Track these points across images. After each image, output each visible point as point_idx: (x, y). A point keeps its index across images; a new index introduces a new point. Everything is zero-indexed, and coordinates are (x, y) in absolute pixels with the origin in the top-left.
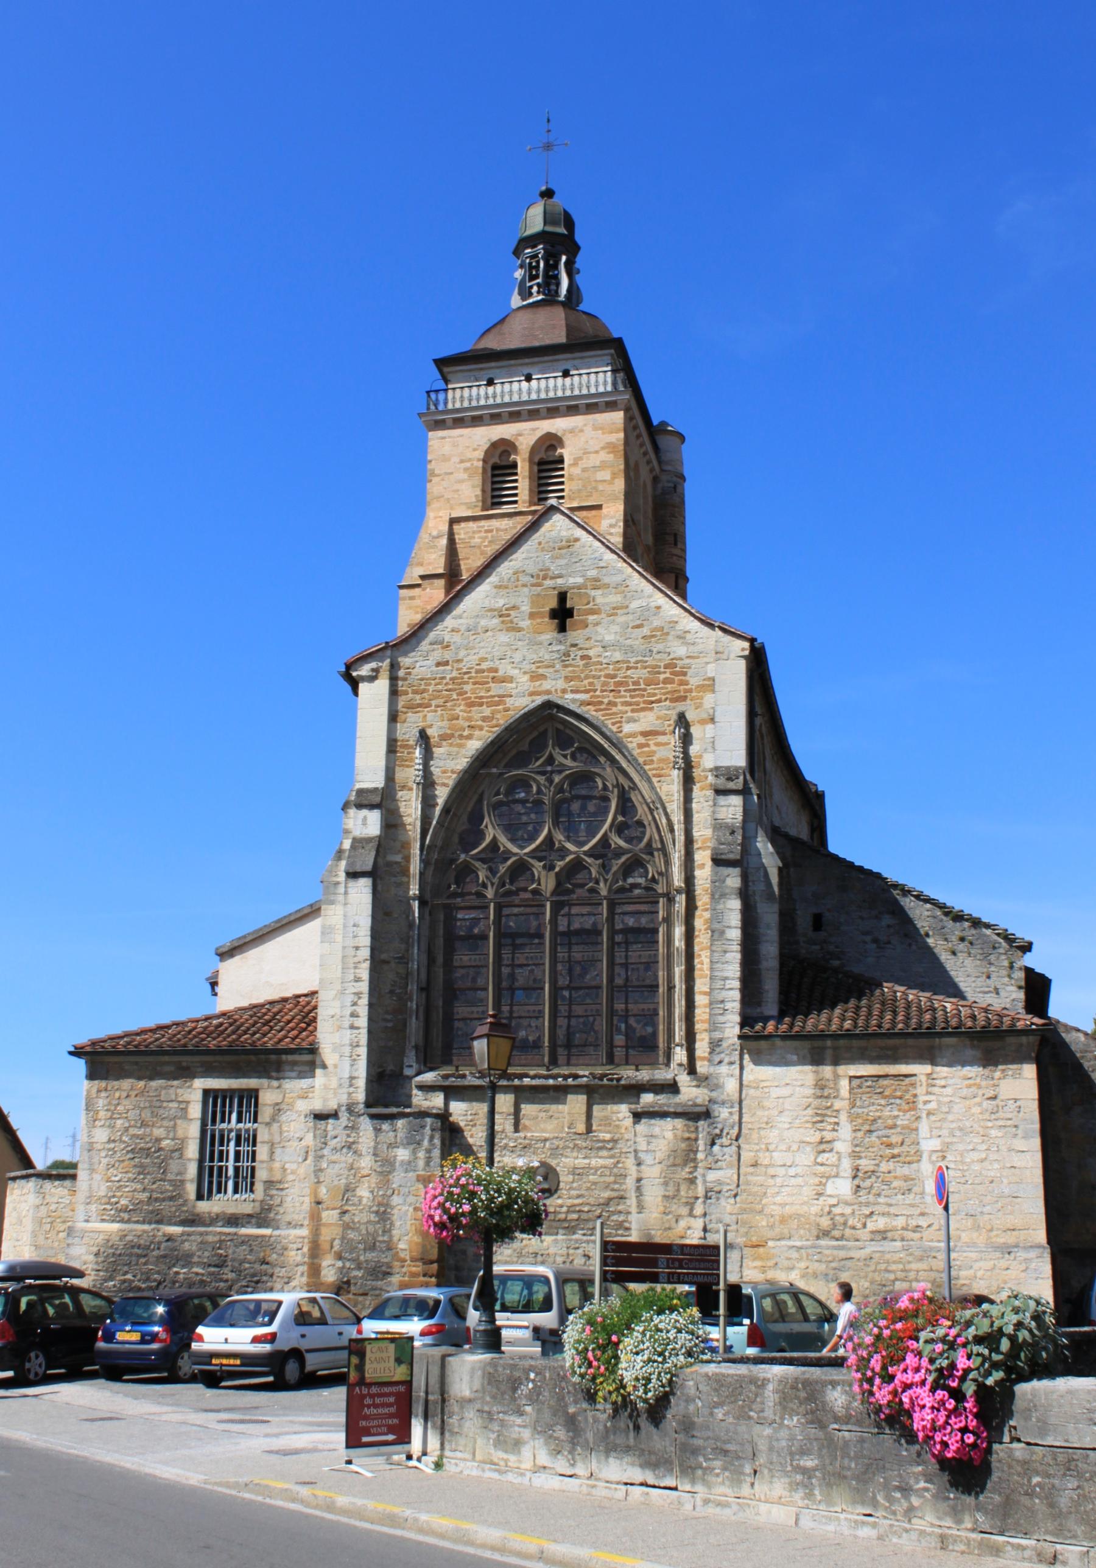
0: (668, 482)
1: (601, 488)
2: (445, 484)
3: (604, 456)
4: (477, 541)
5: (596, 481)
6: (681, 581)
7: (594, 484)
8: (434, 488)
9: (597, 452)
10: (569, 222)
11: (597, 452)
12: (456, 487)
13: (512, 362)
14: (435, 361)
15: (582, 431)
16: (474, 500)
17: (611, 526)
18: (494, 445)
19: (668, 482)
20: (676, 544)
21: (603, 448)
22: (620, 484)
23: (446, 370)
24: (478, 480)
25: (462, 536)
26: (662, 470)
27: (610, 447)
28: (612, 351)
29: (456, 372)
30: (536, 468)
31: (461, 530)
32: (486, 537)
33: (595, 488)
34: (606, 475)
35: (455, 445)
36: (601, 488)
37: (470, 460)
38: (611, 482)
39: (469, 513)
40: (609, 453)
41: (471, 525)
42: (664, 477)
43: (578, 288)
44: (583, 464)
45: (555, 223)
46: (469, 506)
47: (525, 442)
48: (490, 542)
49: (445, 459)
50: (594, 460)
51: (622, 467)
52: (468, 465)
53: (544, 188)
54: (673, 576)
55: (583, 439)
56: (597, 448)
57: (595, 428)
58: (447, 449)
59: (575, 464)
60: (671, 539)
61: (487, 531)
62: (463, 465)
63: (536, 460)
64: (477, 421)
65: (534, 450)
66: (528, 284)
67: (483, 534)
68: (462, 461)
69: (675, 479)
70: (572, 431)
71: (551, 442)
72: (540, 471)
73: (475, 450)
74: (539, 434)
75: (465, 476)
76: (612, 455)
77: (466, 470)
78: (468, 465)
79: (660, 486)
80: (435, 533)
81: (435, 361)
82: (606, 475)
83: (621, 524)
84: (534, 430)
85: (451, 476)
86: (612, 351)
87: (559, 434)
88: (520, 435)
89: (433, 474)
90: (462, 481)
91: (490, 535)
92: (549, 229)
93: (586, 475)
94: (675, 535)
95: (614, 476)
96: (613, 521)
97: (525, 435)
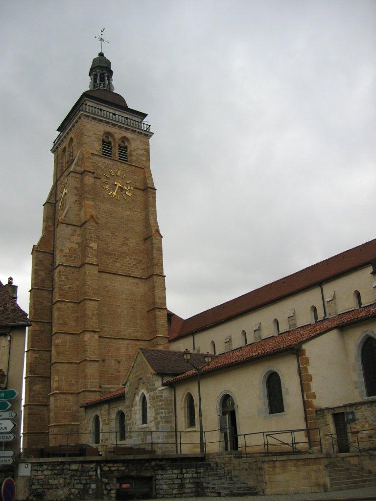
4: (100, 165)
9: (141, 150)
11: (141, 150)
12: (93, 142)
15: (136, 140)
16: (99, 149)
29: (89, 101)
33: (141, 162)
36: (143, 162)
37: (98, 134)
46: (97, 151)
62: (95, 136)
68: (94, 134)
70: (133, 139)
74: (122, 135)
75: (96, 140)
77: (96, 138)
78: (97, 136)
97: (118, 134)
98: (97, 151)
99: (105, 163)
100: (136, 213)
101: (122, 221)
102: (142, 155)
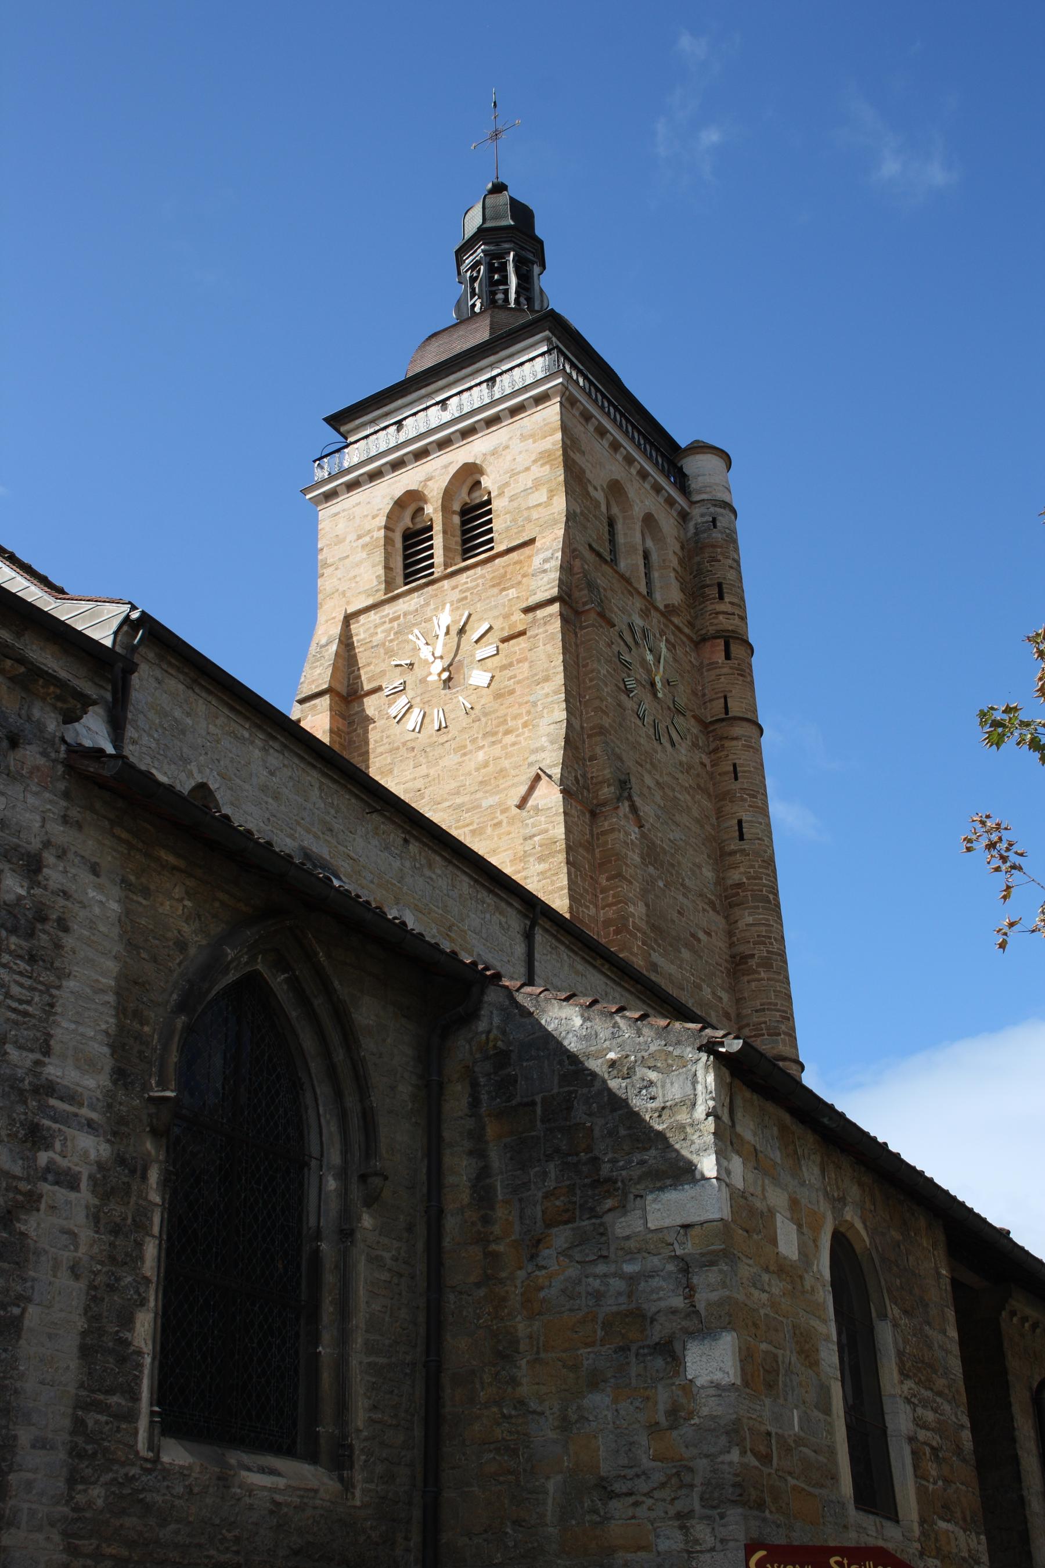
0: (702, 515)
1: (535, 515)
2: (339, 574)
3: (541, 471)
5: (529, 508)
6: (736, 649)
7: (526, 514)
8: (326, 583)
9: (527, 469)
10: (522, 214)
11: (527, 469)
12: (352, 574)
13: (423, 391)
14: (325, 420)
15: (507, 447)
16: (375, 583)
17: (545, 561)
18: (400, 504)
19: (702, 515)
20: (721, 597)
21: (535, 462)
22: (560, 504)
23: (343, 429)
24: (379, 556)
25: (362, 636)
26: (693, 503)
27: (545, 457)
28: (547, 333)
30: (456, 519)
31: (360, 630)
32: (392, 628)
33: (529, 520)
34: (541, 496)
35: (351, 519)
36: (535, 515)
38: (548, 504)
39: (370, 602)
40: (542, 465)
41: (373, 616)
42: (696, 512)
43: (541, 291)
44: (508, 492)
45: (496, 218)
46: (368, 593)
47: (436, 486)
48: (396, 633)
49: (339, 540)
50: (525, 481)
51: (562, 478)
52: (367, 539)
53: (490, 186)
54: (722, 642)
55: (509, 458)
56: (527, 464)
57: (523, 438)
58: (341, 526)
59: (501, 494)
60: (714, 592)
61: (392, 621)
63: (457, 507)
64: (375, 476)
65: (448, 495)
66: (470, 303)
67: (387, 626)
68: (359, 537)
69: (712, 509)
71: (470, 475)
72: (464, 523)
73: (374, 518)
76: (548, 467)
77: (364, 546)
78: (367, 539)
79: (691, 525)
80: (323, 641)
81: (325, 420)
82: (541, 496)
83: (559, 554)
84: (446, 467)
85: (347, 561)
86: (547, 333)
87: (478, 462)
88: (429, 479)
89: (326, 565)
90: (358, 565)
91: (395, 624)
92: (488, 225)
93: (515, 504)
94: (720, 585)
95: (551, 494)
96: (548, 554)
97: (433, 476)
98: (368, 593)
99: (398, 617)
100: (510, 739)
101: (458, 801)
102: (537, 485)
